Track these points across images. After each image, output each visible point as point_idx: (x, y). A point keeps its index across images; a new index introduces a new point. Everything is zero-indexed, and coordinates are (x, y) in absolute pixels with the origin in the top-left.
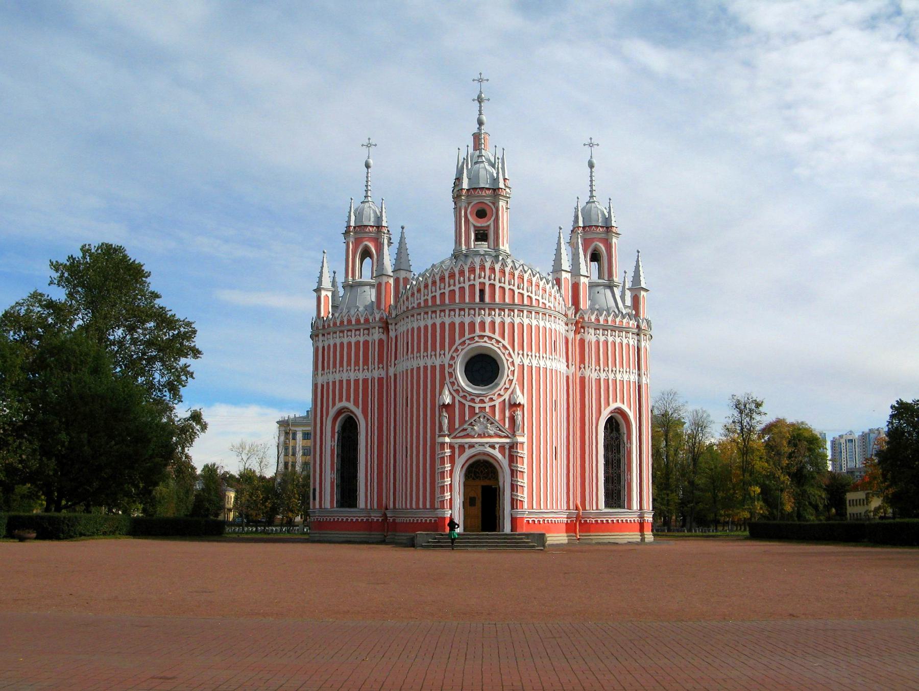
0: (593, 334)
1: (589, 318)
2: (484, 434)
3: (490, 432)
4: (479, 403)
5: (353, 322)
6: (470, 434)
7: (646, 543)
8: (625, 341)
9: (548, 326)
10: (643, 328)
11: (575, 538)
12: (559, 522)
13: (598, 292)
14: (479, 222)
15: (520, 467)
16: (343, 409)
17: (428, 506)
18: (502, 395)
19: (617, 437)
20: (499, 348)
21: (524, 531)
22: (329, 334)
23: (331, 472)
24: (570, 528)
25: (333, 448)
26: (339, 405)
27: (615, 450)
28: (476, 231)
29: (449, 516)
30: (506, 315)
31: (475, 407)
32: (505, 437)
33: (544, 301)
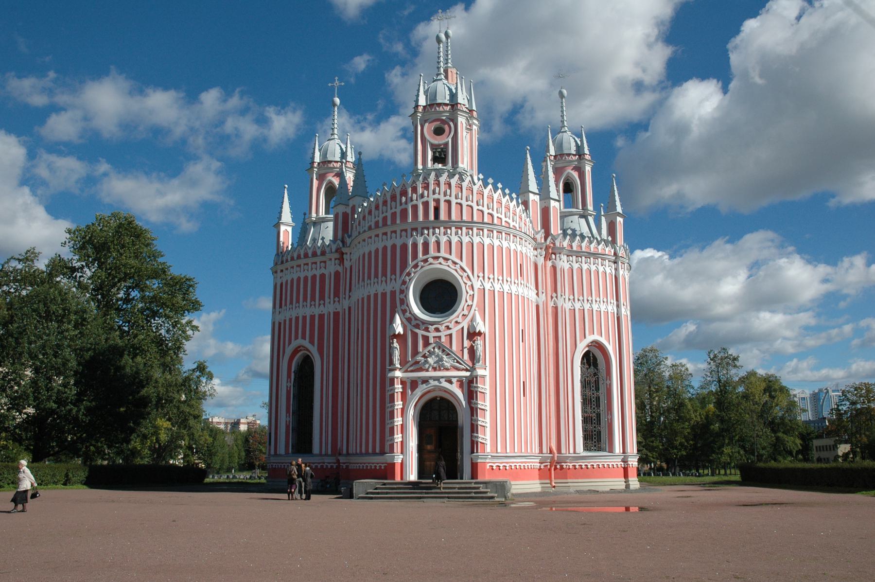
0: (566, 261)
1: (560, 243)
5: (310, 255)
7: (632, 490)
8: (601, 269)
9: (513, 247)
10: (620, 255)
11: (549, 485)
12: (530, 467)
13: (572, 222)
14: (436, 139)
15: (480, 404)
16: (299, 347)
17: (378, 451)
19: (595, 373)
20: (456, 270)
21: (487, 478)
22: (287, 269)
23: (286, 414)
24: (544, 474)
25: (289, 389)
26: (295, 344)
27: (593, 387)
28: (433, 149)
29: (400, 461)
30: (464, 234)
32: (463, 370)
33: (507, 220)
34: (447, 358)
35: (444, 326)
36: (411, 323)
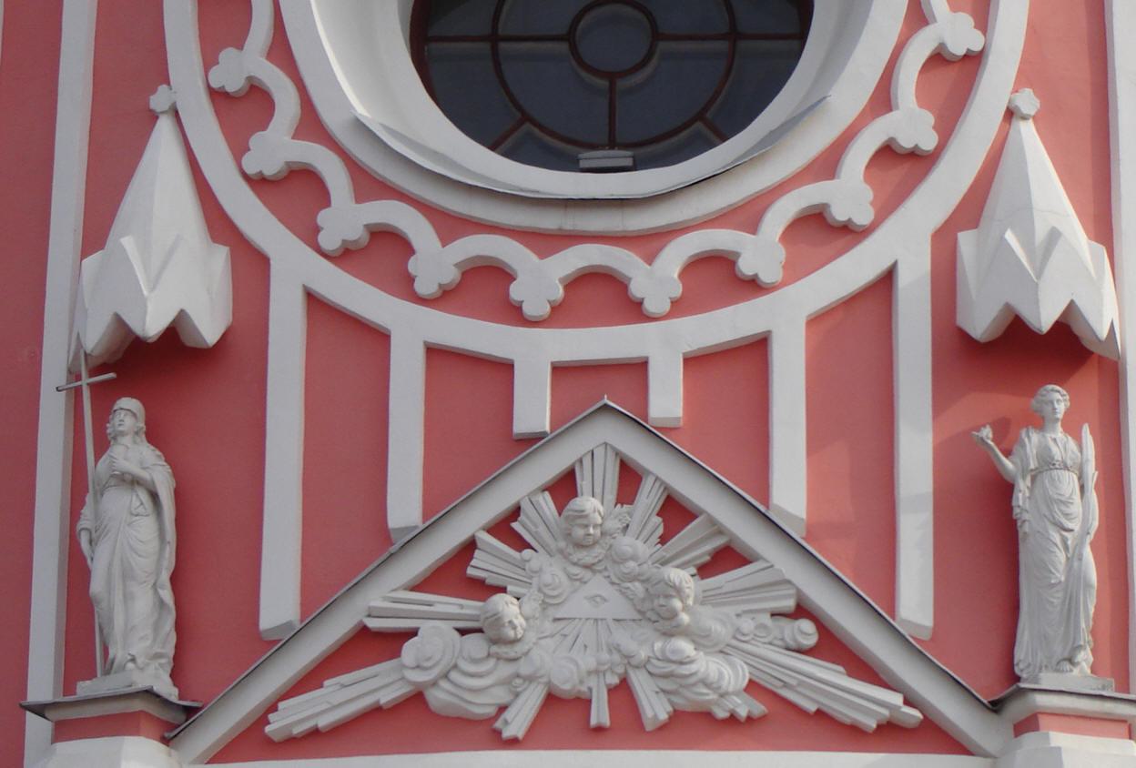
2: (622, 692)
3: (707, 665)
4: (559, 315)
6: (439, 698)
18: (849, 234)
31: (505, 368)
34: (704, 600)
35: (676, 255)
36: (310, 235)
